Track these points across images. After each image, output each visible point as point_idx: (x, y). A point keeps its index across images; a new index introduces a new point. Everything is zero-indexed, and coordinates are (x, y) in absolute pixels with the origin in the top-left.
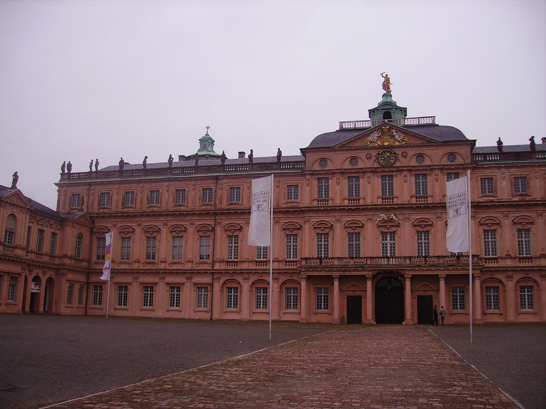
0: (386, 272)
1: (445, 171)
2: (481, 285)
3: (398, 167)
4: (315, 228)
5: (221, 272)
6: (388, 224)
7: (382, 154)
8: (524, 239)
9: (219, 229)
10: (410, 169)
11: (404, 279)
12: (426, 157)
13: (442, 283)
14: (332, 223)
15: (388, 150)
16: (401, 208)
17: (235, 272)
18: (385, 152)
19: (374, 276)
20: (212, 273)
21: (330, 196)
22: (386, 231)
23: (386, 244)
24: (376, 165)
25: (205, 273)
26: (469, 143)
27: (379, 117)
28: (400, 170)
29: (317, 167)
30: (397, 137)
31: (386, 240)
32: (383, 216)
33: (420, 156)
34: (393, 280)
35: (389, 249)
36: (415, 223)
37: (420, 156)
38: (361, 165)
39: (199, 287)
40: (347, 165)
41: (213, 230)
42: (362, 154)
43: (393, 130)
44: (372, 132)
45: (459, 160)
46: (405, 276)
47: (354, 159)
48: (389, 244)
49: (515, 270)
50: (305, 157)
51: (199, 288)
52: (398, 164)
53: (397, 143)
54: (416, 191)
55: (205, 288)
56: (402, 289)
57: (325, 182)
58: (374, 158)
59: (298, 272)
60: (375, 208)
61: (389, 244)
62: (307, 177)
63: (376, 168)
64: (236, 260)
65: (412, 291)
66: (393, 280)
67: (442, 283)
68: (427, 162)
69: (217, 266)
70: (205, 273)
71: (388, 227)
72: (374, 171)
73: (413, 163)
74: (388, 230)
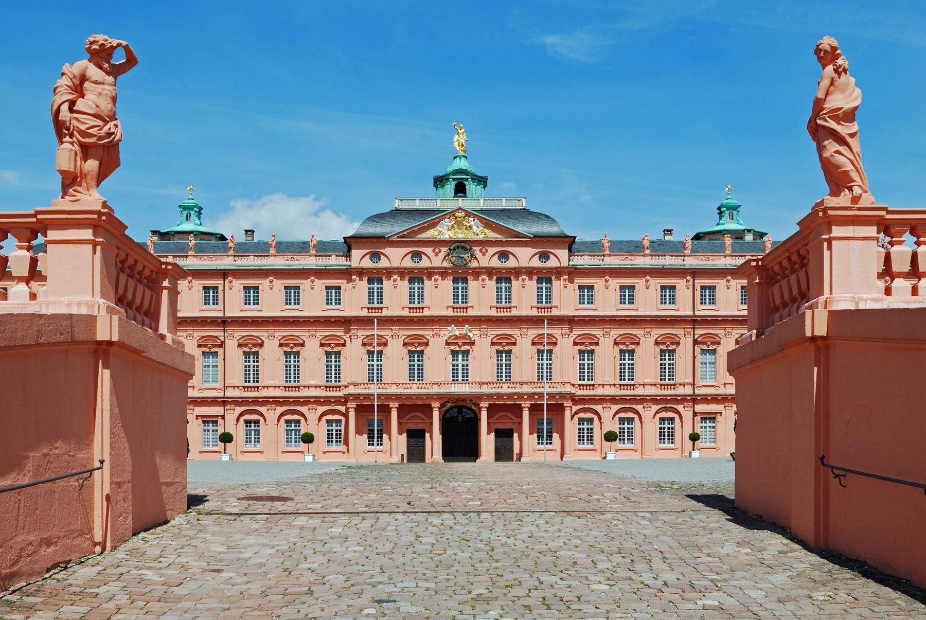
0: (458, 400)
2: (572, 417)
5: (236, 402)
6: (460, 341)
7: (454, 249)
8: (627, 361)
9: (231, 344)
10: (490, 272)
11: (480, 409)
12: (511, 257)
13: (526, 413)
16: (478, 321)
17: (256, 401)
18: (458, 247)
19: (442, 406)
20: (224, 402)
22: (457, 349)
23: (457, 366)
24: (446, 264)
25: (214, 402)
26: (566, 240)
27: (450, 188)
28: (477, 273)
29: (367, 263)
30: (474, 227)
31: (457, 360)
33: (504, 255)
34: (465, 410)
35: (460, 371)
36: (495, 340)
38: (424, 263)
39: (208, 420)
41: (222, 345)
42: (428, 251)
43: (471, 219)
45: (552, 263)
46: (481, 405)
47: (417, 255)
48: (460, 367)
49: (613, 400)
50: (349, 250)
51: (204, 422)
52: (474, 264)
55: (213, 422)
56: (476, 420)
58: (442, 255)
59: (343, 400)
60: (444, 321)
61: (460, 367)
63: (446, 268)
64: (256, 384)
65: (489, 423)
66: (465, 410)
67: (526, 413)
68: (511, 263)
69: (230, 393)
70: (214, 402)
72: (443, 273)
73: (496, 263)
74: (460, 349)
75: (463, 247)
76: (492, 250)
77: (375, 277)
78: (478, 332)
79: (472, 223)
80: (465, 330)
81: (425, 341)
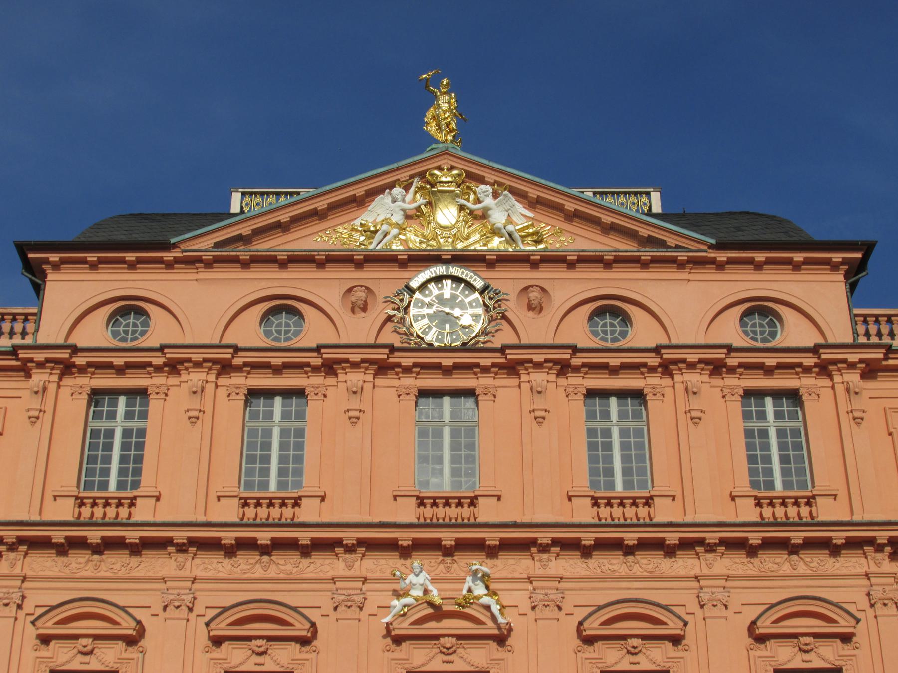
1: (731, 381)
3: (502, 350)
4: (45, 640)
7: (423, 286)
14: (139, 614)
15: (455, 270)
18: (438, 279)
21: (147, 479)
29: (95, 333)
30: (498, 217)
32: (420, 578)
33: (610, 310)
37: (610, 310)
38: (314, 331)
40: (249, 332)
42: (325, 288)
43: (484, 190)
44: (380, 191)
45: (795, 333)
50: (38, 289)
53: (496, 243)
54: (594, 472)
57: (129, 415)
62: (39, 378)
63: (392, 349)
68: (643, 333)
71: (448, 642)
73: (578, 332)
75: (457, 280)
76: (567, 288)
77: (118, 380)
78: (519, 597)
79: (489, 201)
80: (468, 578)
81: (300, 629)
